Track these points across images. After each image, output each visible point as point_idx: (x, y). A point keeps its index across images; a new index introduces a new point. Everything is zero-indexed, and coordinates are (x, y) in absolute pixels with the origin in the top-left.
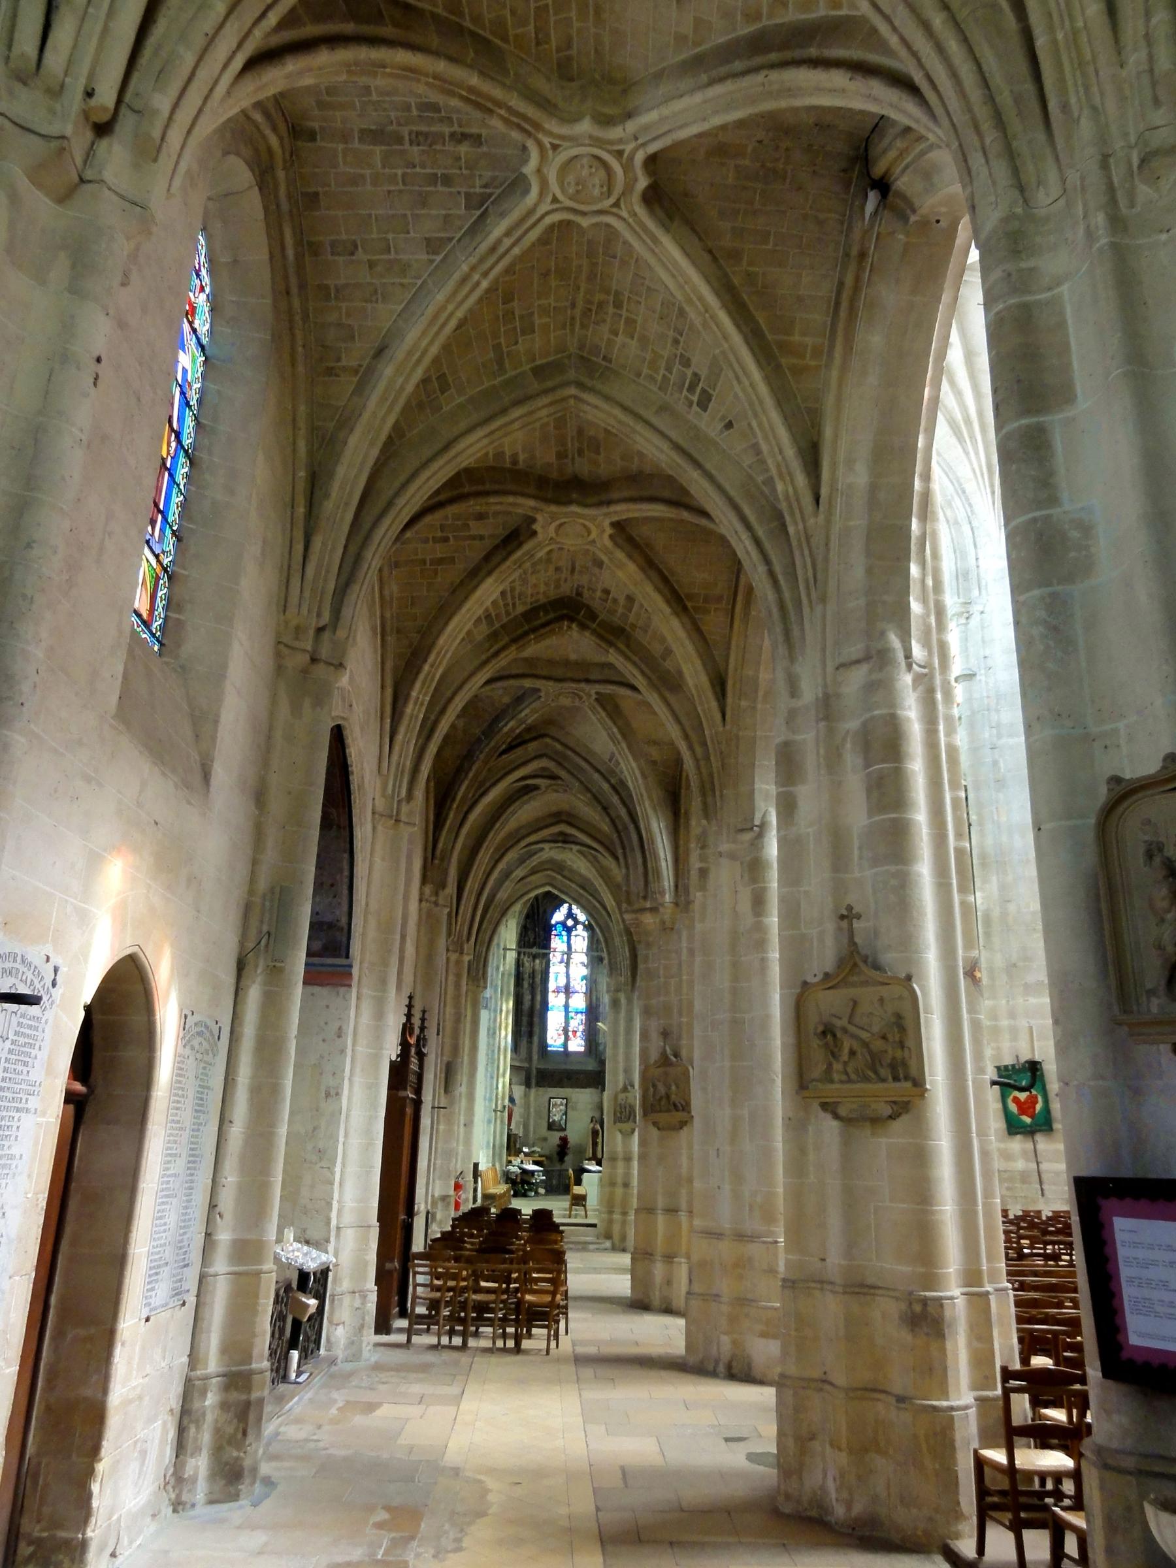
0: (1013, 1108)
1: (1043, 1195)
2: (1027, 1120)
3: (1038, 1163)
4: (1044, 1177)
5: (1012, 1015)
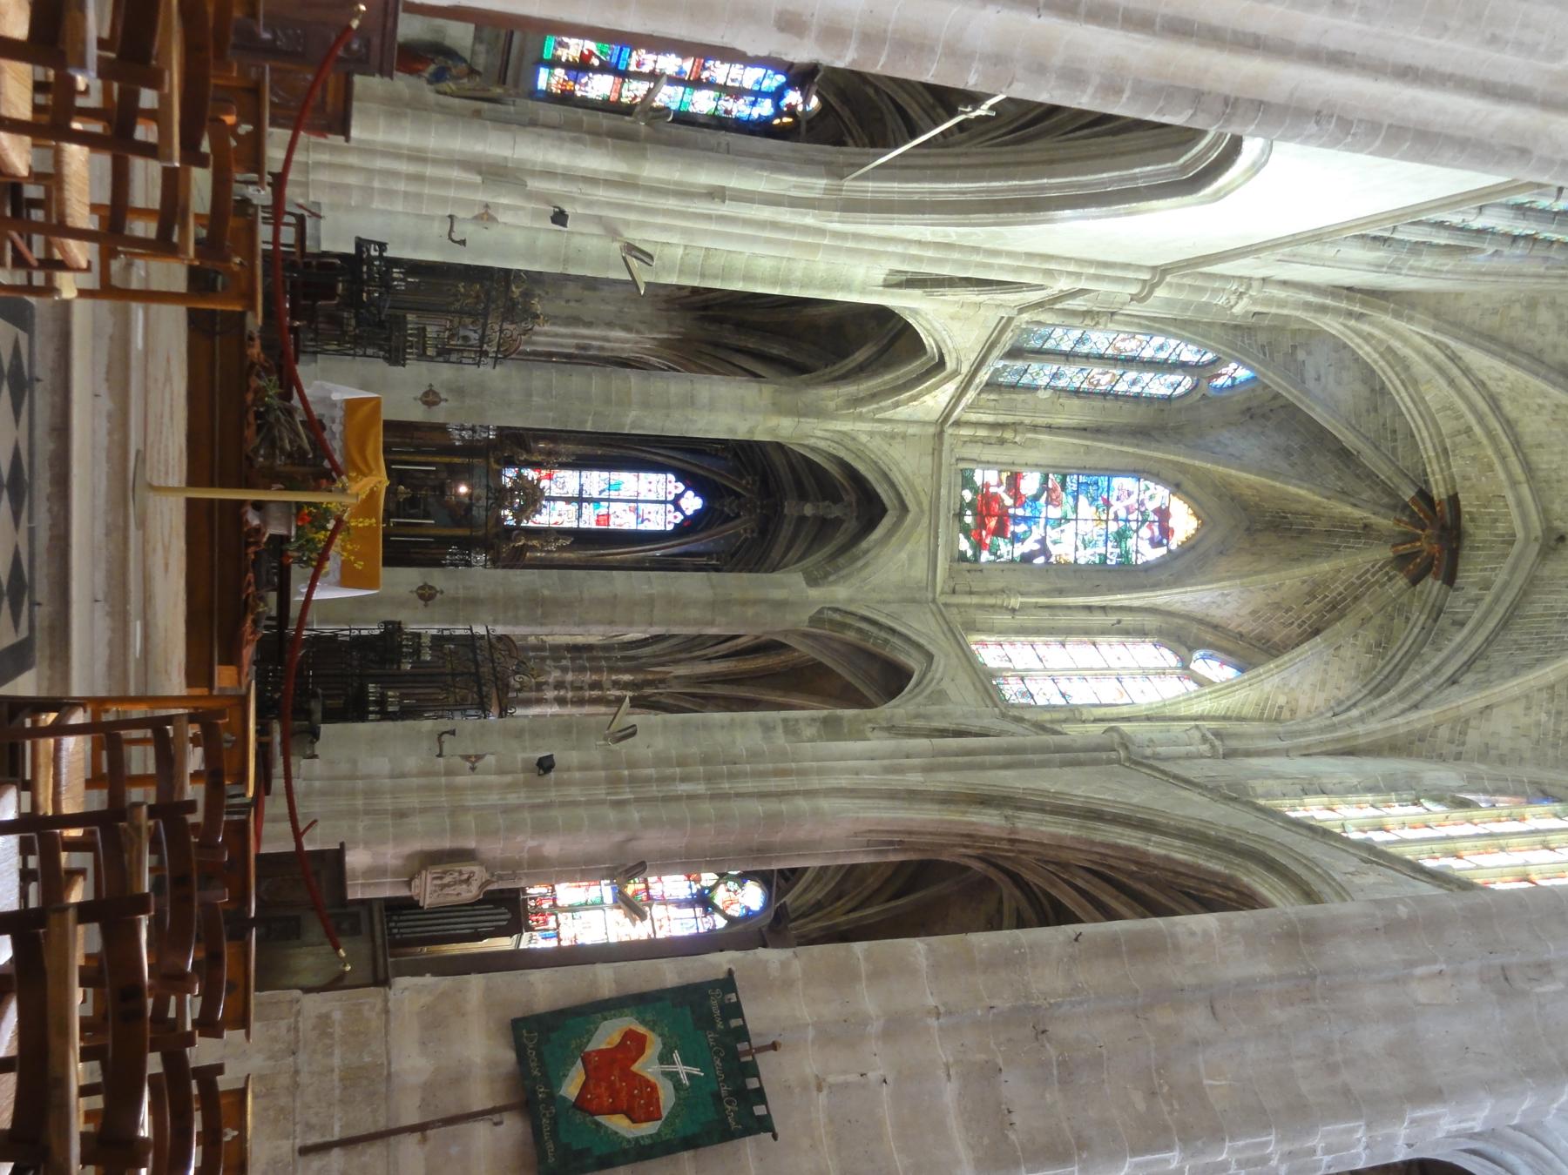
0: (608, 1035)
1: (305, 1151)
2: (571, 1087)
3: (421, 1128)
4: (374, 1152)
5: (898, 1026)
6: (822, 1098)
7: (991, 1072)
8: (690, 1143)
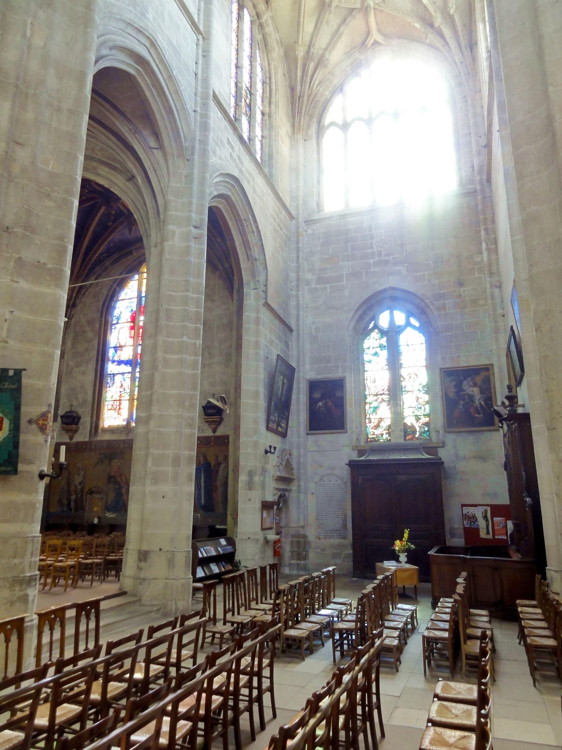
6: (11, 342)
7: (20, 262)
8: (18, 408)
